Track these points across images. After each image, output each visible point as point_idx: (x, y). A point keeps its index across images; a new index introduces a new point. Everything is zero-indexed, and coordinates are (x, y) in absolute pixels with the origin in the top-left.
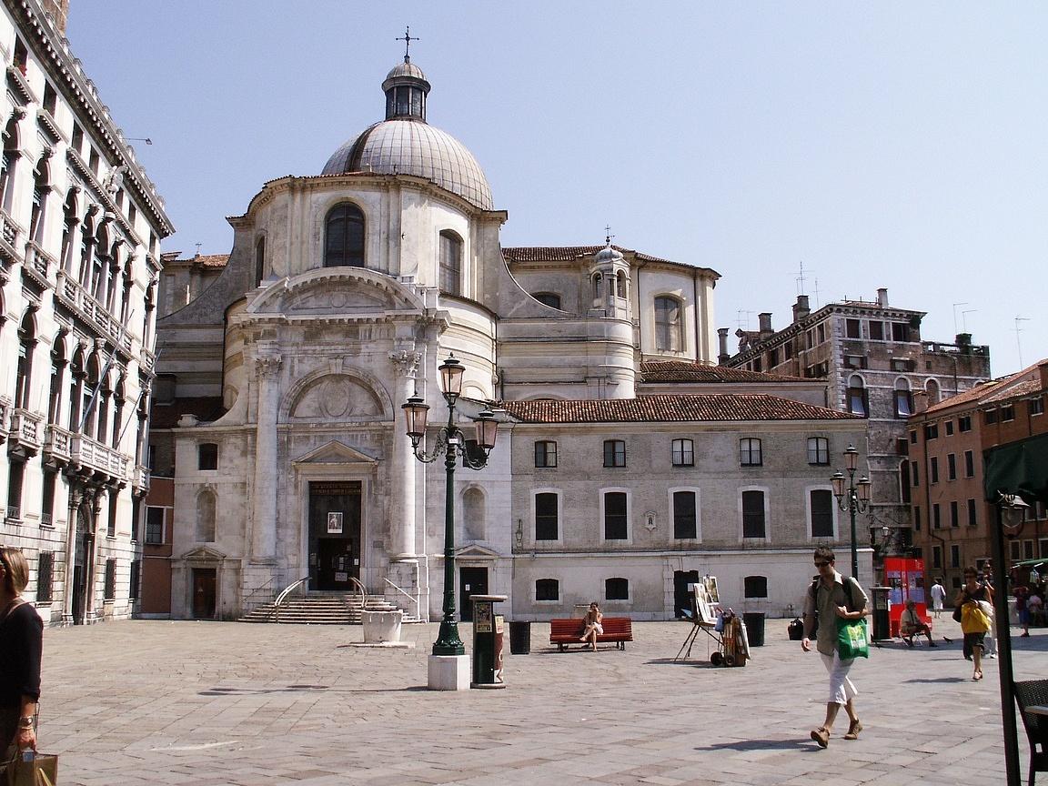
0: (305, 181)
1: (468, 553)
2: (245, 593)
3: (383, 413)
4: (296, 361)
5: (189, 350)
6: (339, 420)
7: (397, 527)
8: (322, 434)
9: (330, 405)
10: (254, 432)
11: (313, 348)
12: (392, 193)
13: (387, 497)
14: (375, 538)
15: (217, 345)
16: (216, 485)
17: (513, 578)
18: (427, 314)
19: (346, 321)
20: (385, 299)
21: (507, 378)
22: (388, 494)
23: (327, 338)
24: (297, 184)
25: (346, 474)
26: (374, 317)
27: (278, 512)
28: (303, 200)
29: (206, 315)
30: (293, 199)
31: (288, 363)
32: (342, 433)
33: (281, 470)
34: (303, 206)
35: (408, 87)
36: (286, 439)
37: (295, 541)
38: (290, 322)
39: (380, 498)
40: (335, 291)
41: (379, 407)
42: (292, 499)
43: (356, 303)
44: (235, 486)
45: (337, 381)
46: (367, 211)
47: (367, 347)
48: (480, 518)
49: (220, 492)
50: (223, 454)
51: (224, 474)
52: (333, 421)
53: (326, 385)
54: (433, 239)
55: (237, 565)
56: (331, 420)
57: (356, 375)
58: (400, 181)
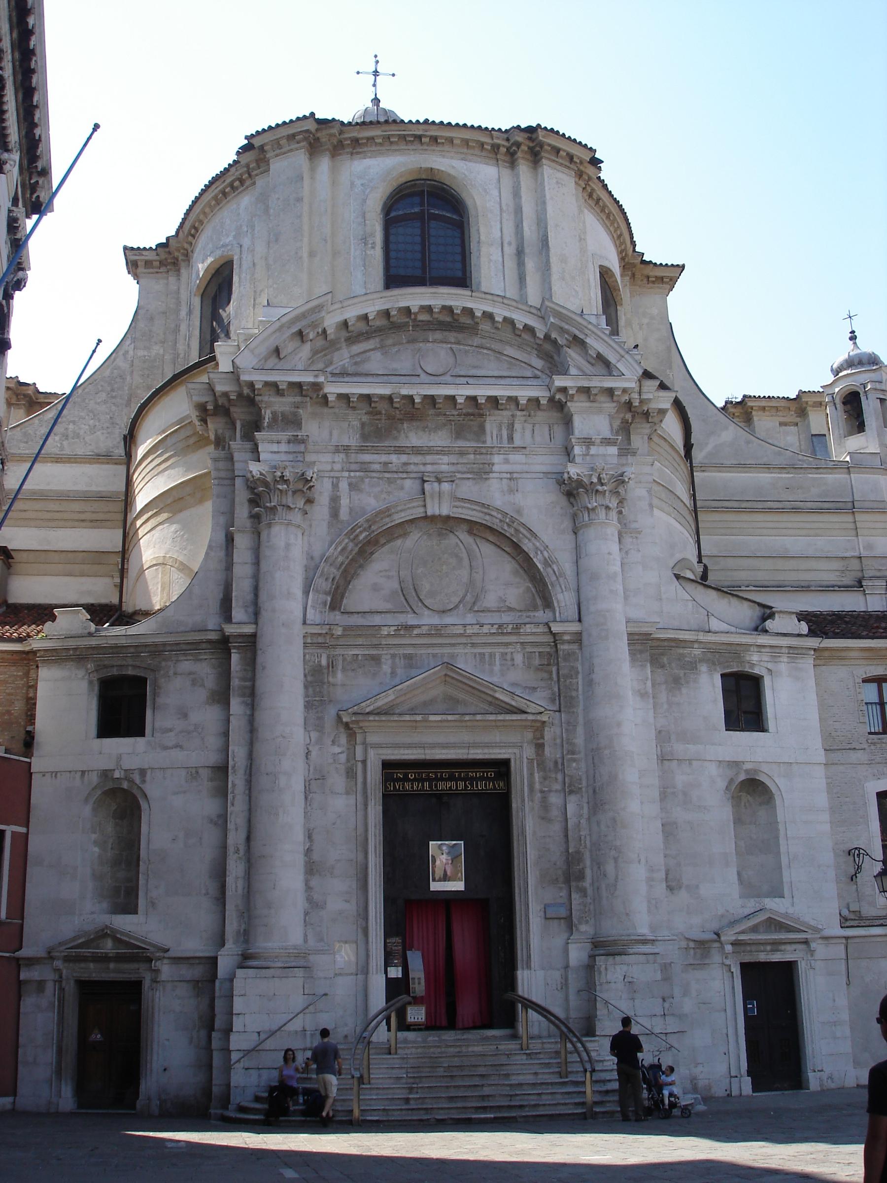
0: (341, 132)
1: (754, 929)
2: (237, 1042)
3: (548, 603)
4: (344, 485)
5: (38, 506)
6: (448, 620)
7: (610, 868)
9: (425, 587)
10: (251, 643)
11: (384, 458)
15: (101, 497)
16: (143, 772)
17: (848, 985)
19: (460, 400)
20: (538, 363)
23: (414, 438)
24: (323, 135)
25: (475, 745)
28: (334, 170)
29: (78, 436)
30: (313, 170)
34: (334, 183)
36: (324, 662)
37: (351, 908)
38: (331, 398)
39: (555, 799)
43: (475, 367)
44: (193, 774)
45: (440, 535)
47: (507, 461)
49: (153, 789)
50: (160, 701)
51: (166, 748)
52: (435, 620)
53: (414, 540)
55: (197, 972)
56: (428, 619)
57: (487, 520)
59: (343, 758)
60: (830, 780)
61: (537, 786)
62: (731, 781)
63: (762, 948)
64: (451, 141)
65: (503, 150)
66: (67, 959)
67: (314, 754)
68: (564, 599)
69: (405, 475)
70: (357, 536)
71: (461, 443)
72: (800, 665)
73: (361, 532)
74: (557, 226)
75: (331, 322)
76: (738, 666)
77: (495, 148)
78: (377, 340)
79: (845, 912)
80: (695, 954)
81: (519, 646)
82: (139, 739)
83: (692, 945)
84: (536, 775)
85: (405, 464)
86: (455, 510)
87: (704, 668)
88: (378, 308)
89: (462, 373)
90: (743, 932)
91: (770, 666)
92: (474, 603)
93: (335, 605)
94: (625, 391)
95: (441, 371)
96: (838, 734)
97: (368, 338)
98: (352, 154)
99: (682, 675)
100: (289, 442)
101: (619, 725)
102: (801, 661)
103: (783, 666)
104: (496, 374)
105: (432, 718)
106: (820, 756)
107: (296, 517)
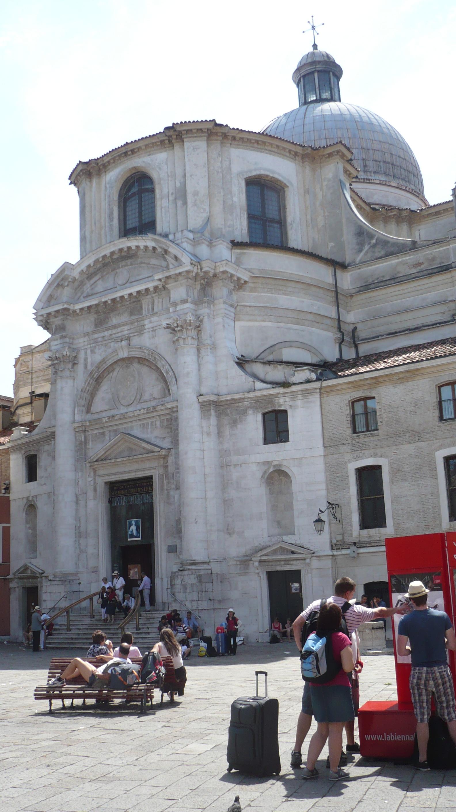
1: (275, 552)
4: (89, 352)
8: (115, 428)
11: (102, 334)
12: (177, 147)
13: (178, 492)
14: (170, 542)
16: (36, 496)
18: (201, 269)
19: (126, 297)
21: (362, 334)
22: (178, 488)
23: (114, 321)
26: (150, 285)
27: (78, 519)
30: (91, 187)
31: (82, 355)
32: (134, 424)
33: (80, 474)
35: (313, 73)
36: (83, 439)
38: (78, 311)
39: (172, 493)
40: (119, 268)
41: (167, 390)
42: (91, 504)
43: (139, 275)
46: (154, 175)
47: (151, 322)
48: (290, 507)
53: (117, 372)
54: (235, 189)
56: (123, 410)
58: (180, 132)
59: (92, 482)
60: (329, 465)
61: (165, 487)
62: (265, 472)
63: (279, 563)
64: (139, 149)
65: (167, 142)
66: (20, 578)
67: (80, 483)
68: (173, 388)
69: (111, 341)
70: (94, 376)
71: (133, 317)
72: (310, 400)
73: (95, 373)
74: (191, 176)
75: (76, 274)
76: (271, 407)
77: (162, 142)
78: (100, 274)
79: (334, 541)
80: (240, 567)
81: (158, 417)
82: (35, 482)
83: (238, 563)
84: (165, 482)
85: (111, 335)
86: (131, 353)
87: (250, 412)
88: (93, 260)
89: (133, 280)
90: (266, 555)
91: (291, 403)
92: (140, 399)
93: (88, 411)
94: (188, 272)
95: (125, 282)
96: (335, 436)
97: (96, 275)
98: (106, 172)
99: (238, 418)
100: (61, 338)
101: (186, 453)
102: (311, 397)
103: (299, 402)
104: (147, 276)
105: (118, 460)
106: (320, 451)
107: (67, 373)
